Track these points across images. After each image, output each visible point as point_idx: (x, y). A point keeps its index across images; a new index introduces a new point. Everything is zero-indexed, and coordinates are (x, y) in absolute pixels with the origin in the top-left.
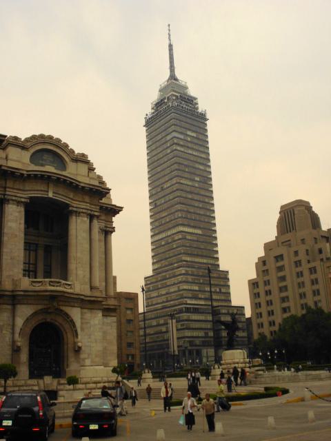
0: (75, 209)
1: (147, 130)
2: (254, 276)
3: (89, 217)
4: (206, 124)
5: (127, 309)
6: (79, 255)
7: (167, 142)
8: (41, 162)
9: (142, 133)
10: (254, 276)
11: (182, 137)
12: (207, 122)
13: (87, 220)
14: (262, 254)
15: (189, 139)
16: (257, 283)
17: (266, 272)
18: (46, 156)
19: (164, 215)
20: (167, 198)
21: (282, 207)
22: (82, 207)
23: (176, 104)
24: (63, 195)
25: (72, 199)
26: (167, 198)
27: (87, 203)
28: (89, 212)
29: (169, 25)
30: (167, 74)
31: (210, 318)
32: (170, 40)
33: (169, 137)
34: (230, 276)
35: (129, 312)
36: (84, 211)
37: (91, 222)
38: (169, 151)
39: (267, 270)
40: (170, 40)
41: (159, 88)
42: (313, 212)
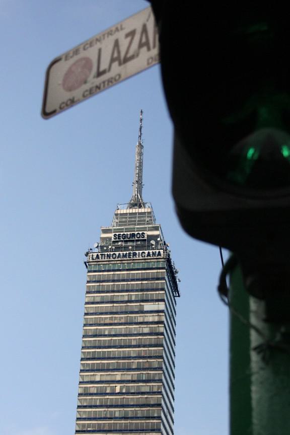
7: (142, 312)
29: (142, 112)
33: (148, 307)
38: (146, 330)
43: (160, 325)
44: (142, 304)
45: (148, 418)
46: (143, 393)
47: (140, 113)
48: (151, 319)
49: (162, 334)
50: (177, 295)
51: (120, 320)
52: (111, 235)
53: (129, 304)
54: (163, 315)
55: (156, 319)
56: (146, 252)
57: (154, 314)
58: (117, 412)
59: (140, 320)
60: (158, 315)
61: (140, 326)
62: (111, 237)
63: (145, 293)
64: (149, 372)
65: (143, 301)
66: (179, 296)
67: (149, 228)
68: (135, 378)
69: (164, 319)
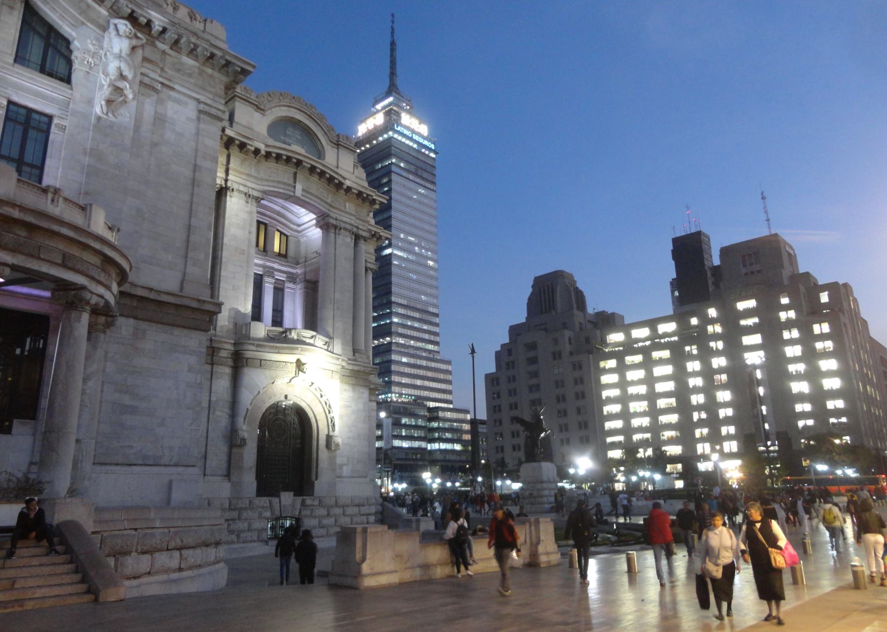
0: (334, 222)
2: (492, 369)
3: (353, 237)
6: (337, 295)
8: (282, 138)
10: (492, 369)
13: (349, 240)
14: (507, 340)
16: (498, 379)
17: (511, 365)
18: (290, 131)
21: (537, 279)
22: (344, 219)
24: (316, 196)
25: (331, 205)
27: (351, 214)
28: (355, 230)
29: (393, 15)
36: (348, 226)
37: (356, 244)
39: (513, 362)
42: (577, 288)
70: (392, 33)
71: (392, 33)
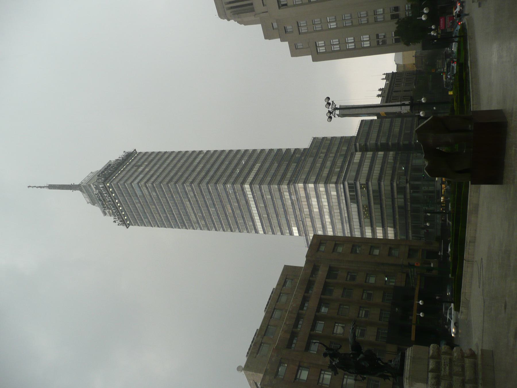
1: (132, 225)
4: (140, 153)
5: (334, 250)
9: (134, 229)
11: (141, 176)
12: (138, 151)
15: (147, 170)
19: (230, 211)
20: (209, 202)
23: (103, 179)
26: (209, 202)
30: (78, 192)
31: (369, 154)
32: (44, 187)
33: (139, 193)
34: (320, 135)
35: (340, 249)
38: (154, 194)
40: (44, 187)
41: (90, 205)
43: (148, 186)
44: (139, 196)
45: (210, 192)
46: (195, 195)
47: (29, 188)
48: (146, 191)
49: (152, 184)
50: (135, 152)
51: (154, 208)
52: (107, 211)
53: (142, 204)
54: (141, 184)
55: (144, 188)
56: (105, 195)
57: (142, 189)
58: (212, 210)
59: (149, 197)
60: (142, 187)
61: (153, 197)
62: (108, 211)
63: (131, 195)
64: (180, 192)
65: (137, 196)
66: (135, 150)
67: (91, 190)
68: (187, 200)
69: (143, 183)
70: (41, 187)
71: (41, 187)
